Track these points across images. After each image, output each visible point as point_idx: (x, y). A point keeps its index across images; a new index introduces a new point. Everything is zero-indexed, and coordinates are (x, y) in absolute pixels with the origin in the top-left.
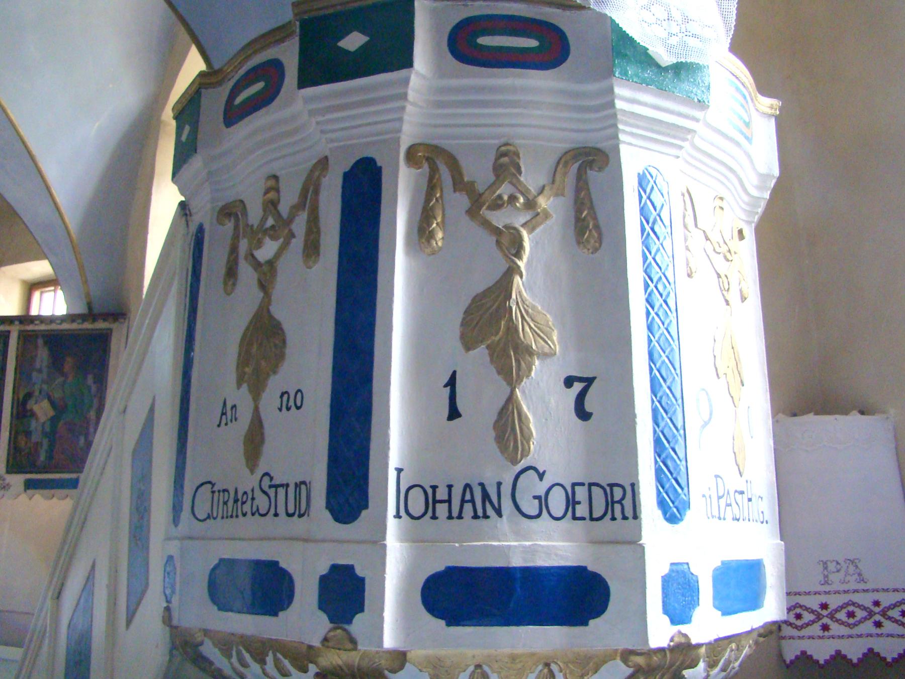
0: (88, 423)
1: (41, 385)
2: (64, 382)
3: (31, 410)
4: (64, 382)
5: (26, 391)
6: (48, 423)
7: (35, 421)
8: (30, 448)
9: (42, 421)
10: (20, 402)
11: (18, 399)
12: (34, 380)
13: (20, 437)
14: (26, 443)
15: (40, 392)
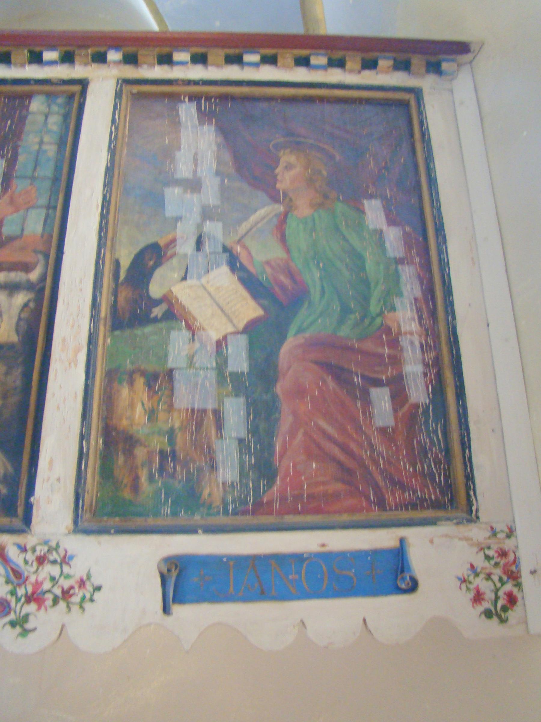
0: (394, 343)
1: (200, 226)
2: (283, 220)
3: (167, 299)
4: (283, 220)
5: (143, 241)
6: (243, 340)
7: (186, 334)
8: (171, 433)
9: (215, 335)
10: (122, 275)
11: (117, 264)
12: (170, 211)
13: (125, 392)
14: (152, 414)
15: (199, 244)
